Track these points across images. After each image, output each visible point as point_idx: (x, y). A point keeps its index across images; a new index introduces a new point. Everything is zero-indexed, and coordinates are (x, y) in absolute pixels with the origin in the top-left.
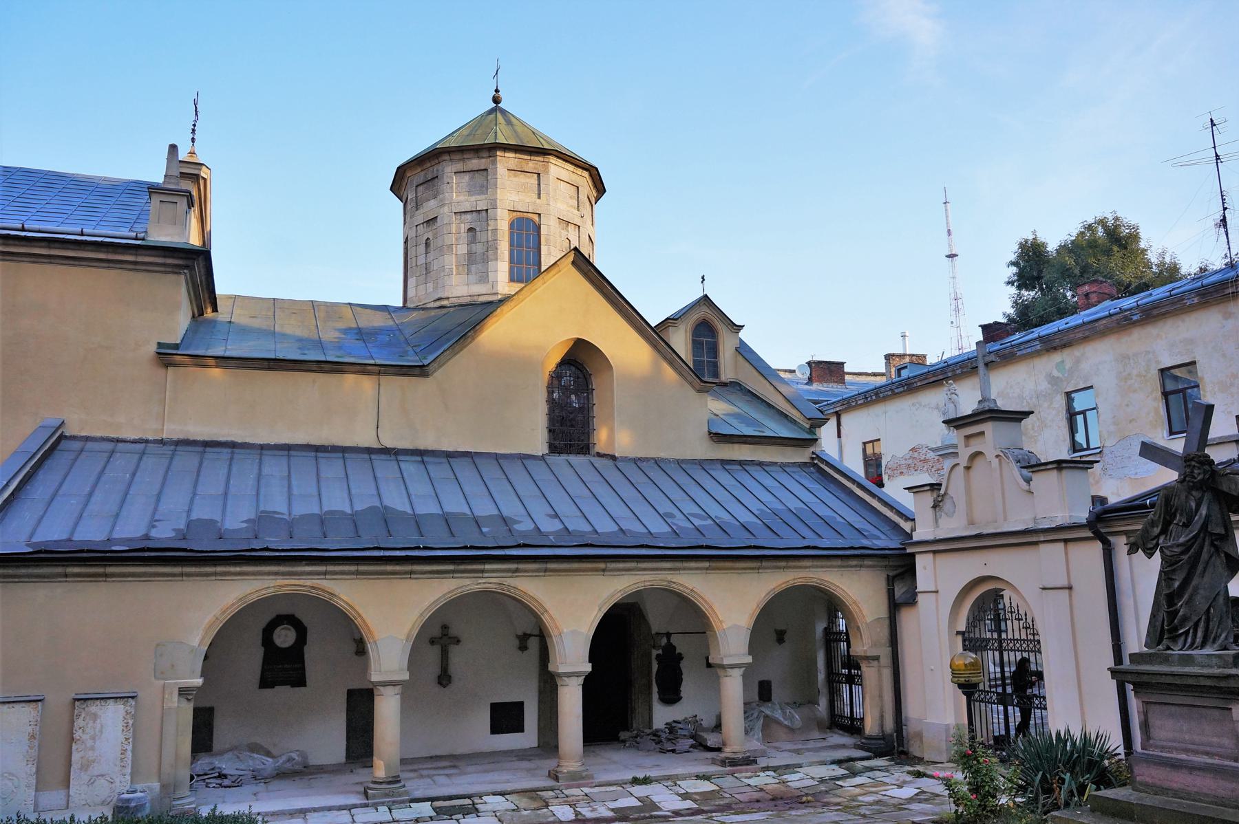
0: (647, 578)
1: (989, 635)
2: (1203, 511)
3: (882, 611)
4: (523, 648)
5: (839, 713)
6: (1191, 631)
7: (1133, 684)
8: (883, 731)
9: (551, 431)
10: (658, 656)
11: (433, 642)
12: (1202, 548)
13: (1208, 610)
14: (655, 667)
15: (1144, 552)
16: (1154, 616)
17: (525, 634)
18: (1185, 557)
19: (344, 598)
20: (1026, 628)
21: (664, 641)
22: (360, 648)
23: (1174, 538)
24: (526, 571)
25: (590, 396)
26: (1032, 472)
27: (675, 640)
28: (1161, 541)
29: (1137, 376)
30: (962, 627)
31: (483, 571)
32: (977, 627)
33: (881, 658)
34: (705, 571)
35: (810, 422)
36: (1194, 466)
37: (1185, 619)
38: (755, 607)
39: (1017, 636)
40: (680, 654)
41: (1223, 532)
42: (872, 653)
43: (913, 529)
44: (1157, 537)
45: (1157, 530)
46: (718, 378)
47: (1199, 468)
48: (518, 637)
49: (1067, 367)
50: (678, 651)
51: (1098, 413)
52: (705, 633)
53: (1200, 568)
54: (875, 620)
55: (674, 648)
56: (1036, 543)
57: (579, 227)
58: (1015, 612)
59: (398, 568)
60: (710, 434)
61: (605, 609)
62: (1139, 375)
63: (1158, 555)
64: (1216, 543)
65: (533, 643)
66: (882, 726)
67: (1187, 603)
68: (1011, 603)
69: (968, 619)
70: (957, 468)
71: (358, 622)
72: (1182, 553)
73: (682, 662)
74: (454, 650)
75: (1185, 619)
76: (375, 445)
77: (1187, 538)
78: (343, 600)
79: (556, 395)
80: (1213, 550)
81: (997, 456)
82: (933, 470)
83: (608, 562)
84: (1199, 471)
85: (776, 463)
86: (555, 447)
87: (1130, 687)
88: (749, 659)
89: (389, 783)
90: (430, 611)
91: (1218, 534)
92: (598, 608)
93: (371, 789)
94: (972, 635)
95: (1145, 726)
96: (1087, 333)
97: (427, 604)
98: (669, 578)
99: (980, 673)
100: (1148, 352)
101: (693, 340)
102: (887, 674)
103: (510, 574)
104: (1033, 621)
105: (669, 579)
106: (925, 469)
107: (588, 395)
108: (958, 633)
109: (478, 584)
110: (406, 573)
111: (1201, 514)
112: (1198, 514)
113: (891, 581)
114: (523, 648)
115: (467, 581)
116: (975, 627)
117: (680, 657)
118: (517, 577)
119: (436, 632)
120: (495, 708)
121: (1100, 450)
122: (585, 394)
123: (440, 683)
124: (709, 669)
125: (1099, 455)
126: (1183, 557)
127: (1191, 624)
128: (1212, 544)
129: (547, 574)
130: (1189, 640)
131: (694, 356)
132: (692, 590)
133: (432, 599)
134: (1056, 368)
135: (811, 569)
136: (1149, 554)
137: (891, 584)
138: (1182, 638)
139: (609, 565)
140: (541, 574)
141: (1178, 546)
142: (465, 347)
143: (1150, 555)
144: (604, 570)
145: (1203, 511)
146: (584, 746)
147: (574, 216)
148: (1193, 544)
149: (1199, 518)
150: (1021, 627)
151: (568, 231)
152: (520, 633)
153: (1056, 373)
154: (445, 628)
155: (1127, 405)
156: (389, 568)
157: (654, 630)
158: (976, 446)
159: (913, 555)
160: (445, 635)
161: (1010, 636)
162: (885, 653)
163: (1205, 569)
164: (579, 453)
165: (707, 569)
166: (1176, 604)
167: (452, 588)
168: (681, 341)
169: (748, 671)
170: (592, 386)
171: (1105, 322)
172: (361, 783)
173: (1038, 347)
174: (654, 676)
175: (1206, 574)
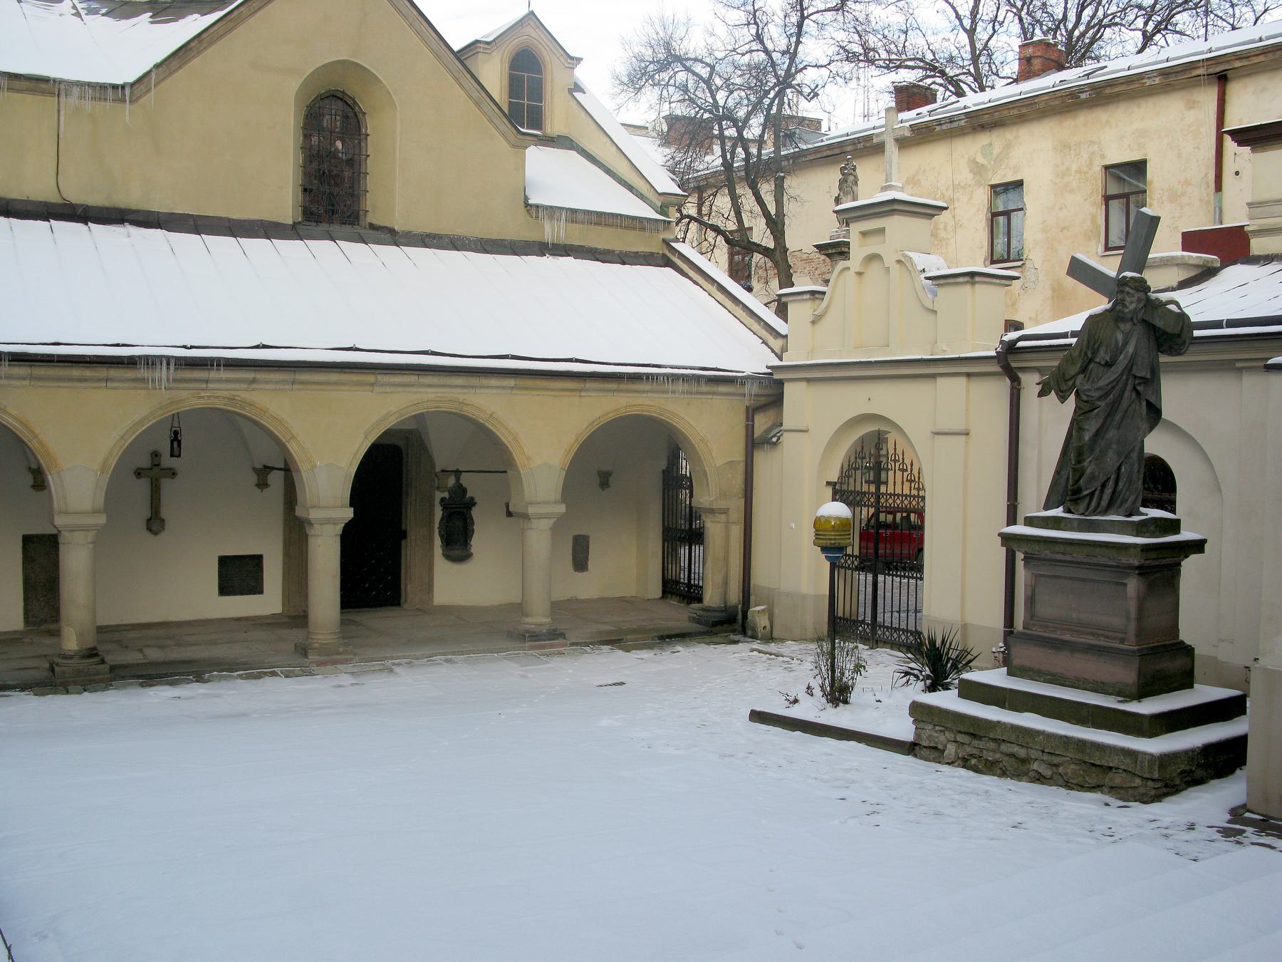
0: (431, 396)
1: (865, 488)
2: (1131, 349)
3: (738, 454)
4: (262, 484)
5: (674, 578)
6: (1097, 493)
7: (1026, 553)
8: (725, 602)
9: (305, 190)
10: (443, 500)
11: (139, 474)
12: (1123, 392)
13: (1119, 468)
14: (438, 513)
15: (1057, 394)
16: (1058, 472)
17: (265, 467)
18: (1102, 404)
19: (14, 412)
20: (911, 481)
21: (451, 481)
22: (39, 481)
23: (1093, 379)
24: (267, 382)
25: (363, 144)
26: (938, 285)
27: (465, 480)
28: (1078, 383)
29: (1076, 171)
30: (834, 477)
32: (851, 476)
33: (730, 510)
34: (509, 391)
35: (662, 198)
36: (1128, 293)
38: (573, 441)
39: (898, 491)
40: (472, 498)
41: (1149, 376)
42: (722, 504)
43: (784, 349)
44: (1074, 376)
46: (542, 129)
47: (1133, 296)
48: (254, 469)
49: (995, 153)
50: (468, 495)
51: (1025, 214)
52: (505, 472)
53: (1118, 417)
54: (727, 463)
55: (465, 491)
56: (933, 376)
58: (899, 461)
59: (88, 373)
60: (526, 207)
61: (372, 438)
62: (1079, 171)
63: (1072, 399)
64: (1138, 388)
65: (276, 479)
66: (725, 593)
68: (895, 449)
69: (842, 468)
70: (846, 273)
71: (34, 445)
72: (1100, 398)
73: (473, 508)
74: (166, 484)
75: (1093, 478)
76: (54, 198)
77: (1108, 381)
78: (13, 416)
79: (315, 140)
80: (1134, 395)
81: (899, 262)
82: (817, 273)
83: (379, 374)
84: (1133, 299)
85: (613, 251)
86: (312, 213)
87: (1020, 556)
88: (562, 509)
89: (84, 657)
90: (134, 433)
91: (1141, 378)
92: (363, 436)
93: (57, 665)
94: (845, 487)
95: (1031, 601)
96: (1024, 111)
98: (461, 397)
99: (850, 539)
100: (1093, 143)
101: (510, 74)
102: (737, 531)
103: (244, 386)
104: (919, 474)
105: (461, 401)
106: (806, 271)
107: (360, 143)
108: (828, 483)
109: (200, 397)
110: (100, 380)
111: (1128, 352)
112: (1124, 353)
113: (751, 412)
114: (262, 484)
116: (849, 477)
117: (472, 503)
118: (253, 390)
119: (145, 462)
120: (223, 561)
121: (1022, 262)
122: (356, 141)
123: (149, 529)
124: (510, 518)
125: (1020, 269)
126: (1099, 403)
127: (1098, 484)
128: (1134, 388)
129: (296, 386)
130: (1093, 504)
131: (510, 98)
132: (491, 416)
133: (137, 417)
134: (981, 152)
135: (649, 395)
136: (1061, 397)
137: (750, 417)
138: (1087, 500)
139: (379, 377)
140: (286, 387)
142: (186, 62)
143: (1063, 398)
144: (372, 385)
145: (1131, 349)
146: (341, 613)
148: (1113, 388)
149: (1124, 358)
150: (905, 479)
152: (259, 466)
153: (980, 160)
154: (156, 455)
155: (1061, 209)
157: (438, 469)
158: (873, 246)
159: (780, 383)
160: (155, 465)
161: (890, 490)
162: (737, 505)
164: (345, 224)
165: (512, 388)
166: (1084, 460)
168: (494, 75)
169: (559, 524)
170: (366, 130)
171: (1047, 98)
172: (45, 656)
173: (963, 123)
174: (437, 525)
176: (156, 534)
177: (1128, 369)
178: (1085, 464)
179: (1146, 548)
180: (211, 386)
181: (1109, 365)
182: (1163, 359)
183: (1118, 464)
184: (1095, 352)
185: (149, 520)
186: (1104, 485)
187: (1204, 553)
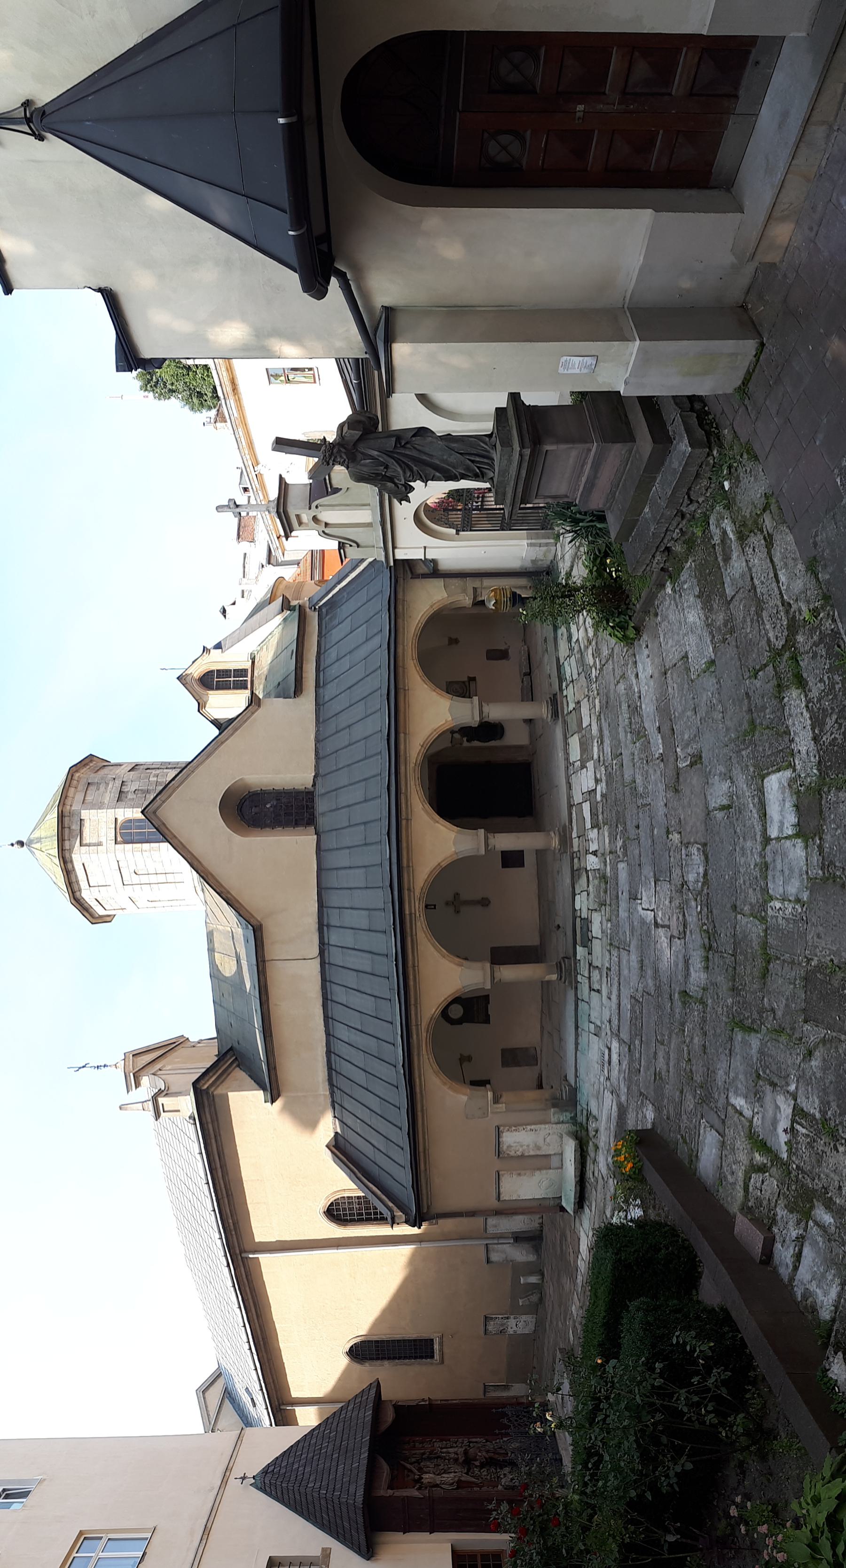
2: (375, 453)
6: (478, 465)
13: (461, 454)
15: (409, 493)
18: (415, 468)
31: (411, 914)
37: (468, 469)
41: (394, 439)
44: (396, 484)
45: (390, 484)
57: (123, 782)
59: (411, 977)
64: (403, 444)
67: (454, 467)
72: (411, 470)
74: (464, 896)
80: (408, 446)
97: (436, 953)
110: (414, 970)
111: (378, 456)
115: (418, 924)
127: (472, 465)
128: (404, 447)
133: (432, 949)
141: (404, 472)
143: (412, 489)
145: (375, 453)
147: (115, 786)
148: (404, 462)
149: (382, 457)
151: (128, 792)
156: (411, 983)
163: (425, 453)
166: (455, 474)
167: (424, 935)
175: (431, 453)
176: (490, 902)
177: (389, 454)
178: (457, 474)
179: (522, 446)
180: (413, 911)
181: (387, 467)
182: (380, 429)
183: (458, 455)
184: (378, 474)
185: (483, 906)
186: (473, 461)
187: (519, 393)
